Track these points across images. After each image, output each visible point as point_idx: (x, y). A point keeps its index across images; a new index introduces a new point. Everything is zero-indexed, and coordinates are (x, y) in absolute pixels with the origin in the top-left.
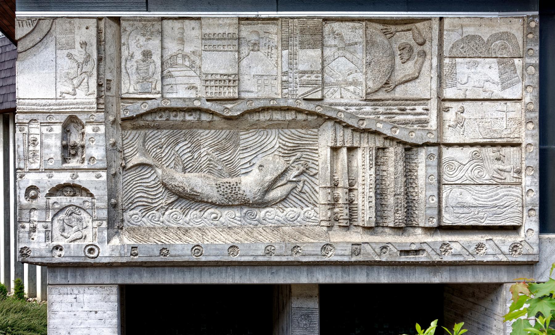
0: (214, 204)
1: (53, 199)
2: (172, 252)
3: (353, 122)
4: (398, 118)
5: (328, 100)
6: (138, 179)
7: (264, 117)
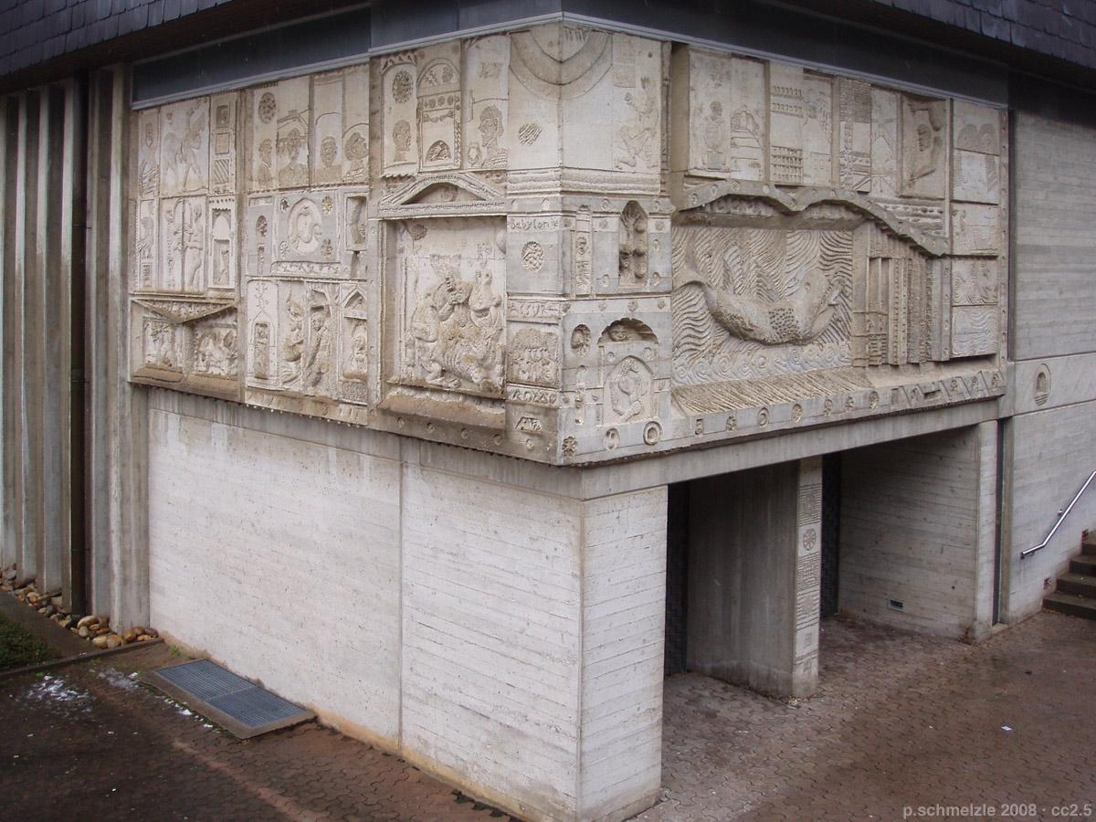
0: (764, 343)
1: (609, 346)
2: (739, 424)
3: (893, 226)
4: (923, 220)
5: (873, 195)
6: (685, 306)
7: (816, 214)
